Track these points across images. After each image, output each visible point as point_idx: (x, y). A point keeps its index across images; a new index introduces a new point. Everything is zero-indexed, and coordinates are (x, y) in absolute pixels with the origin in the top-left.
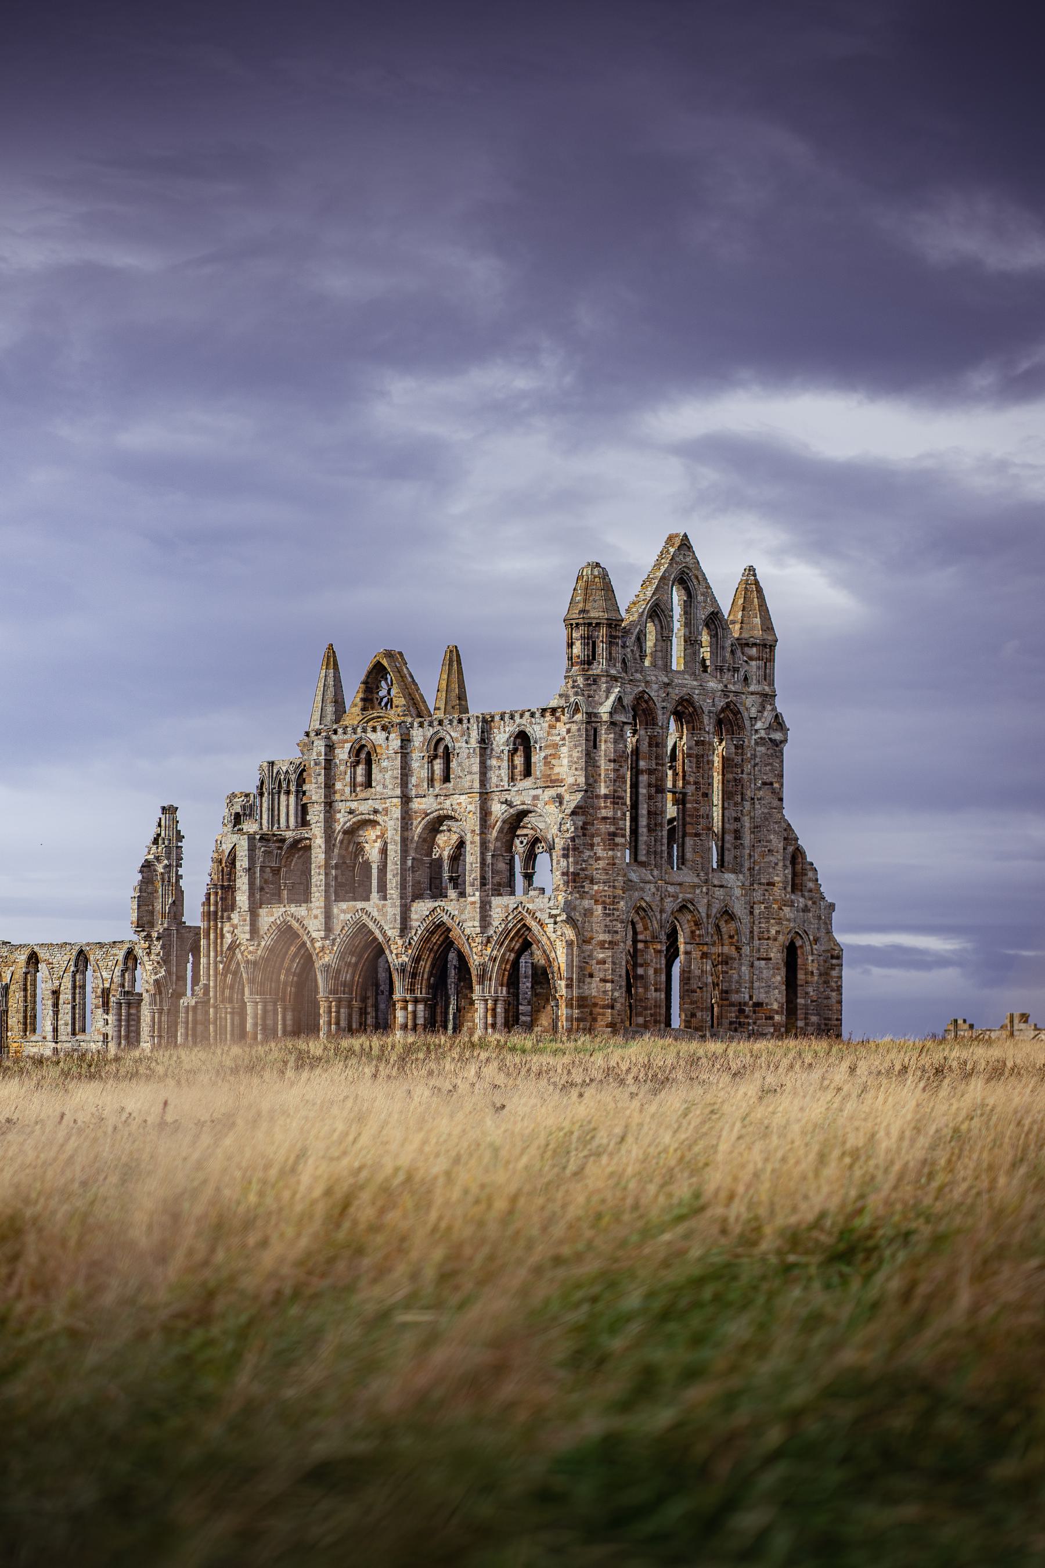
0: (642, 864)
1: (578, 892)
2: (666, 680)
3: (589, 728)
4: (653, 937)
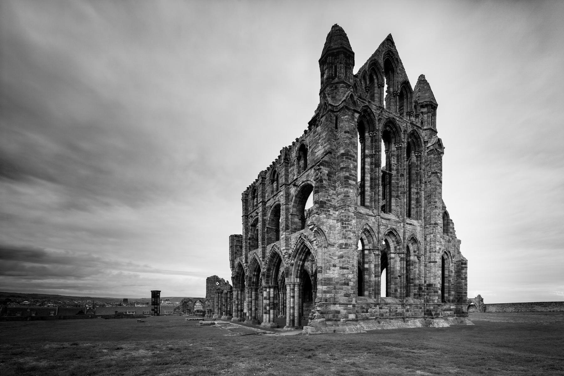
1: (325, 214)
4: (374, 247)
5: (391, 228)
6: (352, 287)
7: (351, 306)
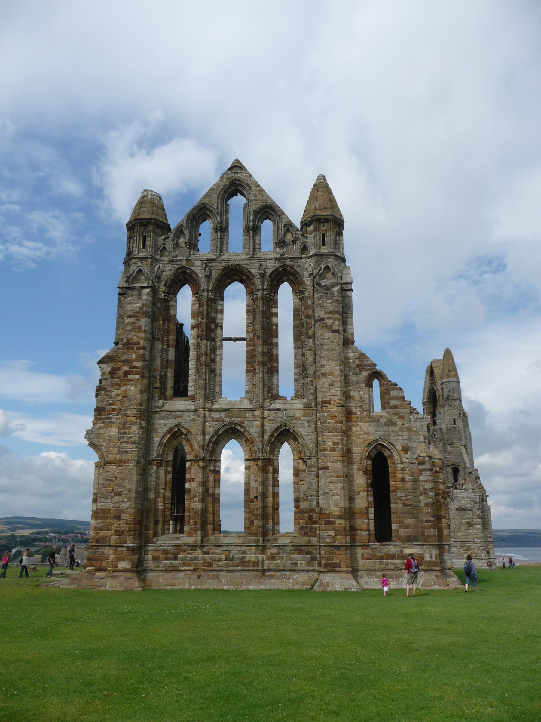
0: (193, 398)
1: (103, 423)
2: (215, 257)
3: (122, 298)
4: (196, 456)
5: (230, 423)
6: (127, 520)
7: (125, 549)
